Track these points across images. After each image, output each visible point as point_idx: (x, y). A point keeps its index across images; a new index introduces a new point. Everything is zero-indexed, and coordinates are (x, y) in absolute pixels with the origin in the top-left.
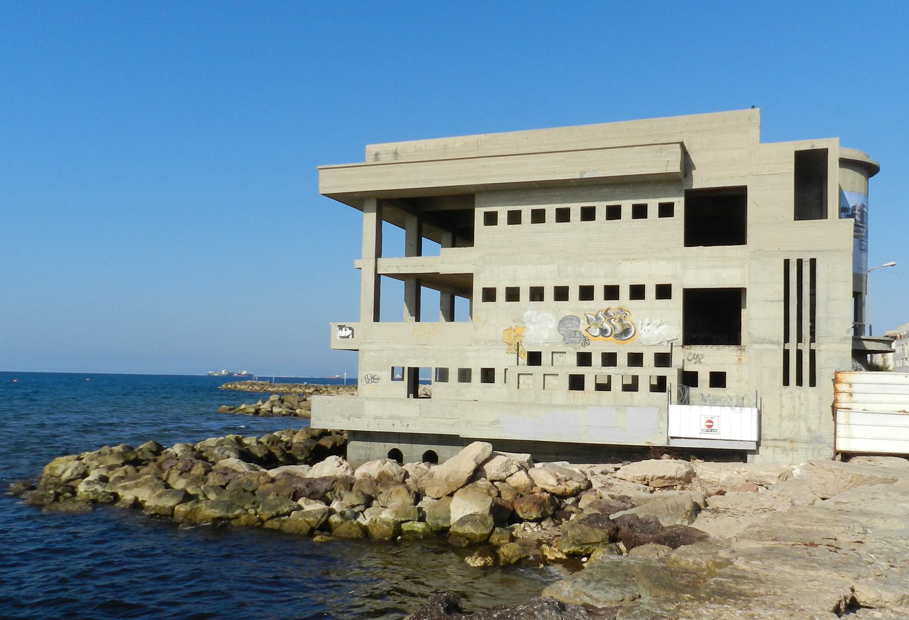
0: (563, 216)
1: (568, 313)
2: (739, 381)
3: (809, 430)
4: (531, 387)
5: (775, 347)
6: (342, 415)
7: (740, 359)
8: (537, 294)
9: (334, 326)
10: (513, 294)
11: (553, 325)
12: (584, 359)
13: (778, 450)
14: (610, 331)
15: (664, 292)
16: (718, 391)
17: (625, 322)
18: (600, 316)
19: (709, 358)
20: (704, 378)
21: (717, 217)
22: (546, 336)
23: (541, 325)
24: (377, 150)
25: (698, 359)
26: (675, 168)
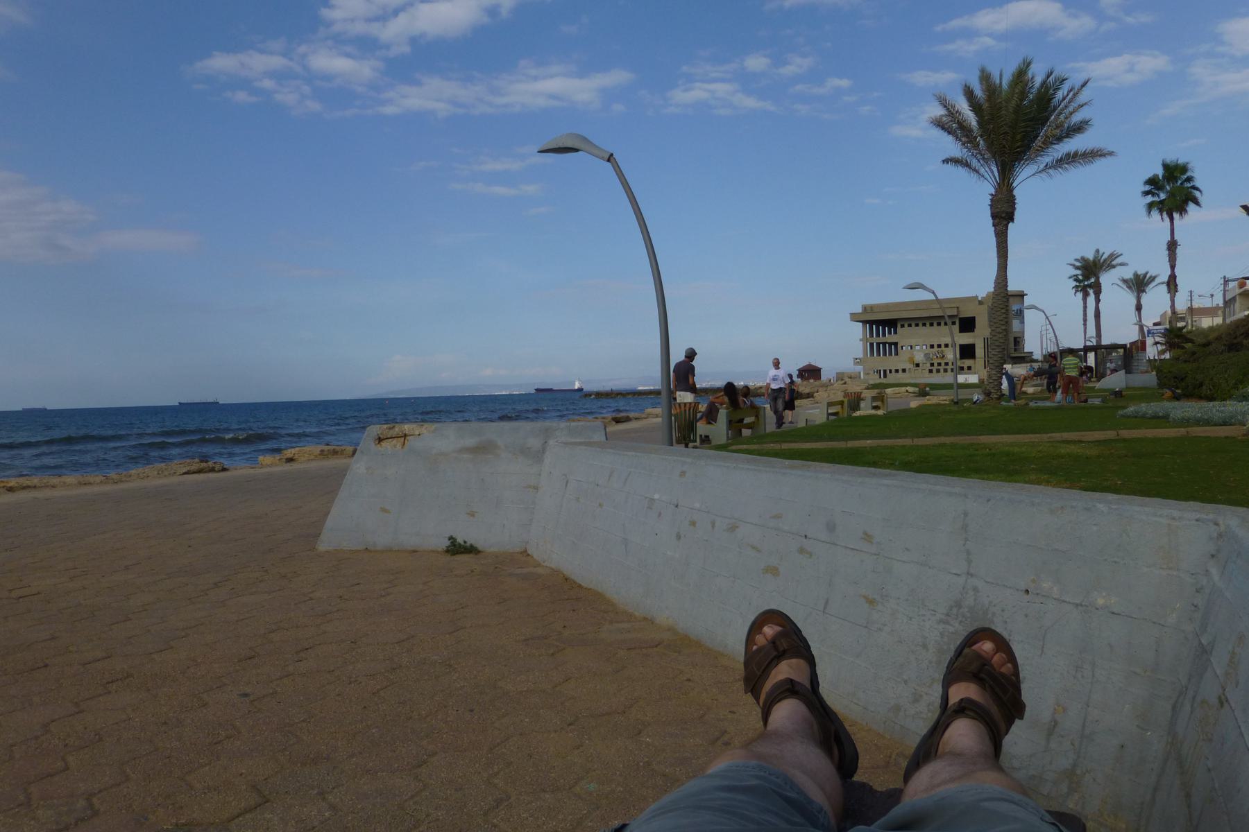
12: (932, 365)
19: (967, 363)
21: (967, 325)
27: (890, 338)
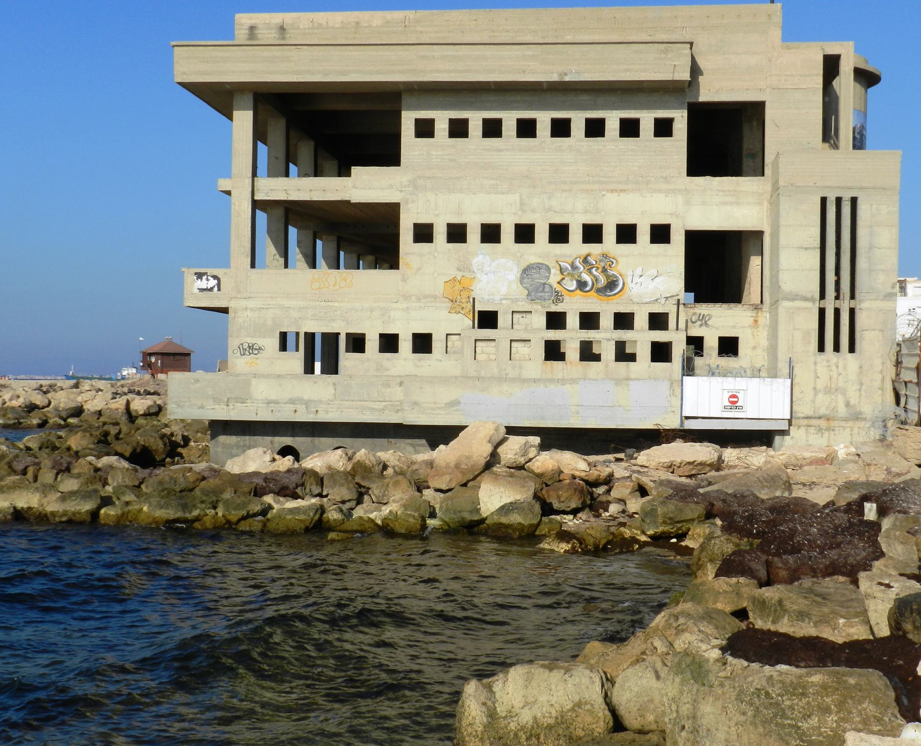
0: (526, 129)
1: (533, 260)
2: (754, 348)
3: (848, 404)
4: (493, 357)
5: (809, 304)
6: (217, 400)
7: (756, 321)
8: (491, 234)
9: (189, 275)
10: (457, 234)
11: (514, 274)
12: (556, 320)
13: (812, 430)
14: (590, 283)
15: (660, 234)
16: (728, 362)
17: (610, 272)
18: (577, 264)
19: (720, 320)
20: (711, 344)
22: (504, 290)
23: (496, 275)
24: (253, 22)
25: (704, 321)
26: (686, 76)
27: (365, 186)
